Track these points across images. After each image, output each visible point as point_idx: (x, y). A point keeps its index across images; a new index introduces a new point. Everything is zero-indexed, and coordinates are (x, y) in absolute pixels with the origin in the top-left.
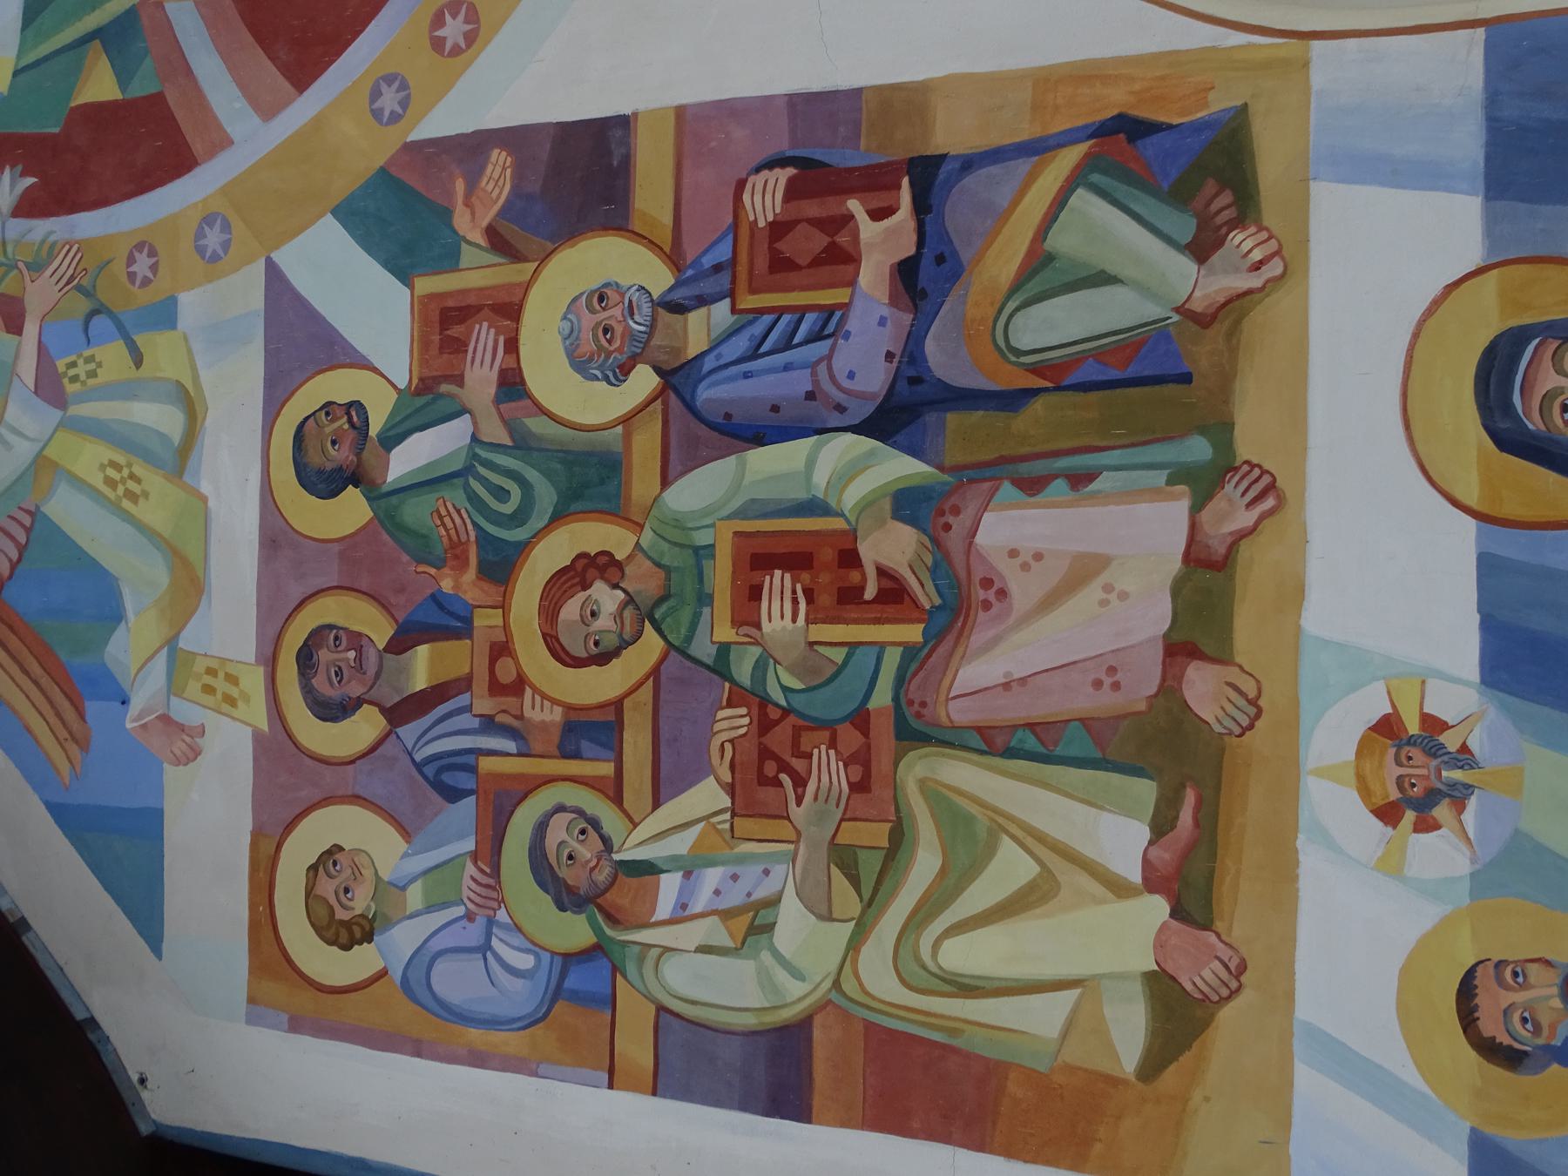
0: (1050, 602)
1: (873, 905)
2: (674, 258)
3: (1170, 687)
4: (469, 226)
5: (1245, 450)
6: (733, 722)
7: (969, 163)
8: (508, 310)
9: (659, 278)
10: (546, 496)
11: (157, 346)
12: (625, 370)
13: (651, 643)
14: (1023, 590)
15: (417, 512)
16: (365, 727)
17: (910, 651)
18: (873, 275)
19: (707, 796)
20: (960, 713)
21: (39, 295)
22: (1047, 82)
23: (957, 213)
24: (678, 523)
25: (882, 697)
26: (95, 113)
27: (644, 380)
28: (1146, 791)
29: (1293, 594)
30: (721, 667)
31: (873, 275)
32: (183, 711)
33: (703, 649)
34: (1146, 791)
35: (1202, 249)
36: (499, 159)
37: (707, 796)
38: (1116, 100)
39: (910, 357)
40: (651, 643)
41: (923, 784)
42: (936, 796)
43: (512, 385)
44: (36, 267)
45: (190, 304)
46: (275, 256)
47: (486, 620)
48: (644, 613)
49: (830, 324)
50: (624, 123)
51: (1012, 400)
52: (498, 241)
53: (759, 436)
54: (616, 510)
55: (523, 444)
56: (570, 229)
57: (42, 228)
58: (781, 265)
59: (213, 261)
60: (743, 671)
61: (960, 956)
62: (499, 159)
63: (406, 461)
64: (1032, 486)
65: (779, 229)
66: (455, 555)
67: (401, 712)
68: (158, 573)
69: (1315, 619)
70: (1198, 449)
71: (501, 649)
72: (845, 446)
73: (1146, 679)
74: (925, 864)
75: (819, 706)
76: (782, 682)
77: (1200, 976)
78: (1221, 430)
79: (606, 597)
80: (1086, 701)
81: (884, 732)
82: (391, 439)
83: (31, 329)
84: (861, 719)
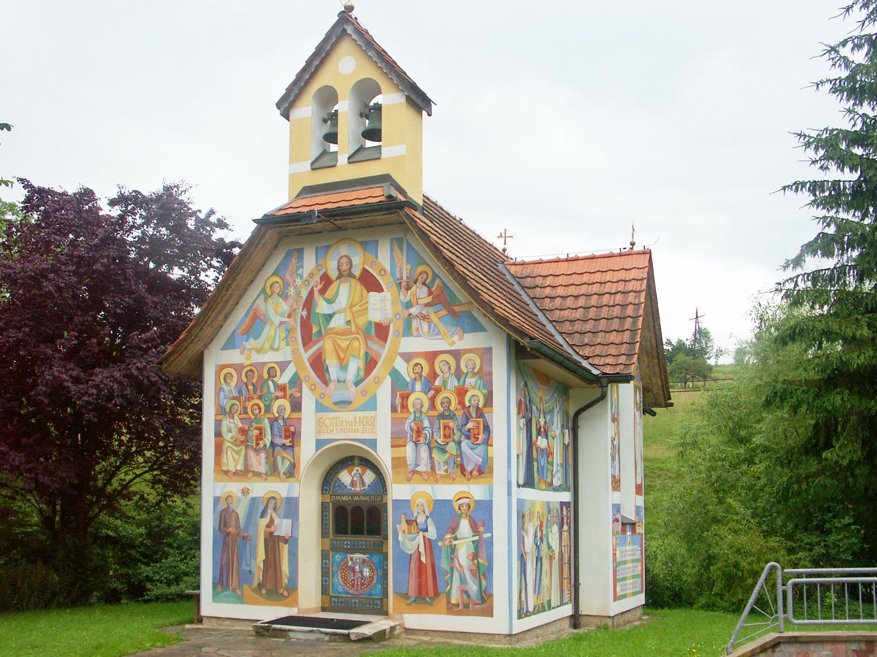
0: (257, 459)
1: (232, 443)
2: (288, 418)
3: (251, 471)
4: (292, 391)
5: (269, 478)
6: (246, 427)
7: (293, 451)
8: (284, 397)
9: (286, 417)
10: (267, 403)
11: (284, 343)
12: (278, 412)
13: (253, 417)
14: (258, 457)
15: (265, 385)
16: (245, 380)
17: (252, 446)
18: (284, 441)
19: (240, 425)
20: (248, 451)
21: (291, 320)
22: (299, 459)
23: (289, 450)
24: (264, 420)
25: (249, 444)
26: (311, 329)
27: (277, 415)
28: (243, 469)
29: (258, 482)
30: (251, 426)
31: (284, 441)
32: (246, 350)
33: (253, 423)
34: (243, 469)
35: (284, 474)
36: (299, 394)
37: (240, 425)
38: (296, 464)
39: (277, 445)
40: (253, 417)
41: (241, 449)
42: (241, 449)
43: (277, 398)
44: (294, 320)
45: (288, 348)
46: (292, 363)
47: (255, 396)
48: (256, 416)
49: (281, 436)
50: (300, 411)
51: (273, 457)
52: (292, 394)
53: (271, 429)
54: (265, 412)
55: (272, 400)
56: (292, 406)
57: (299, 320)
58: (286, 431)
59: (293, 352)
60: (251, 428)
61: (229, 452)
62: (299, 394)
63: (270, 383)
64: (266, 458)
65: (289, 430)
66: (261, 391)
67: (246, 384)
68: (260, 346)
69: (256, 484)
70: (269, 474)
71: (253, 398)
72: (270, 439)
73: (251, 469)
74: (236, 448)
75: (248, 436)
76: (250, 433)
77: (230, 474)
78: (270, 476)
79: (257, 412)
80: (250, 463)
81: (246, 444)
82: (273, 381)
83: (287, 320)
84: (247, 441)
